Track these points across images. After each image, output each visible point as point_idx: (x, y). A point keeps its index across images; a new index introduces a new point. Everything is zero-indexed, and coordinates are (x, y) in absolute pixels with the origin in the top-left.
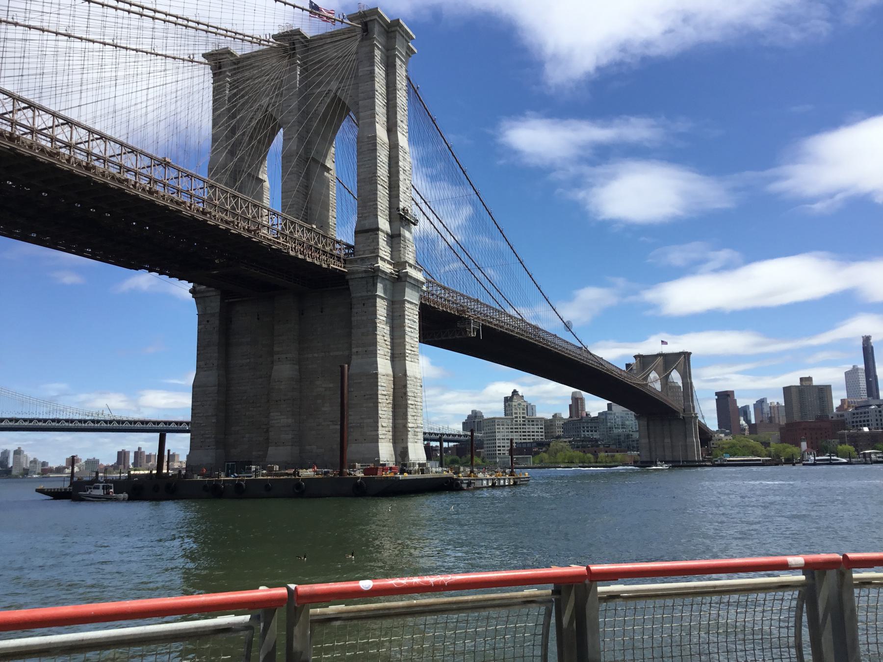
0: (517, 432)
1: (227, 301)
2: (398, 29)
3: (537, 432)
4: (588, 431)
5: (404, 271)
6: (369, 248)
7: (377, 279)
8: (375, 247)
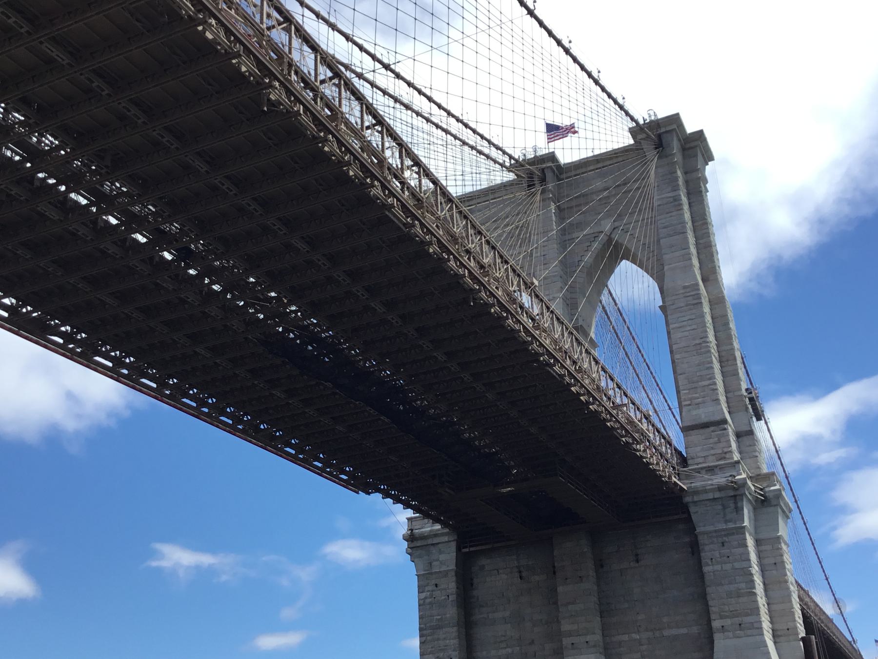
1: (467, 550)
2: (700, 143)
5: (772, 488)
6: (712, 452)
7: (742, 500)
8: (725, 450)
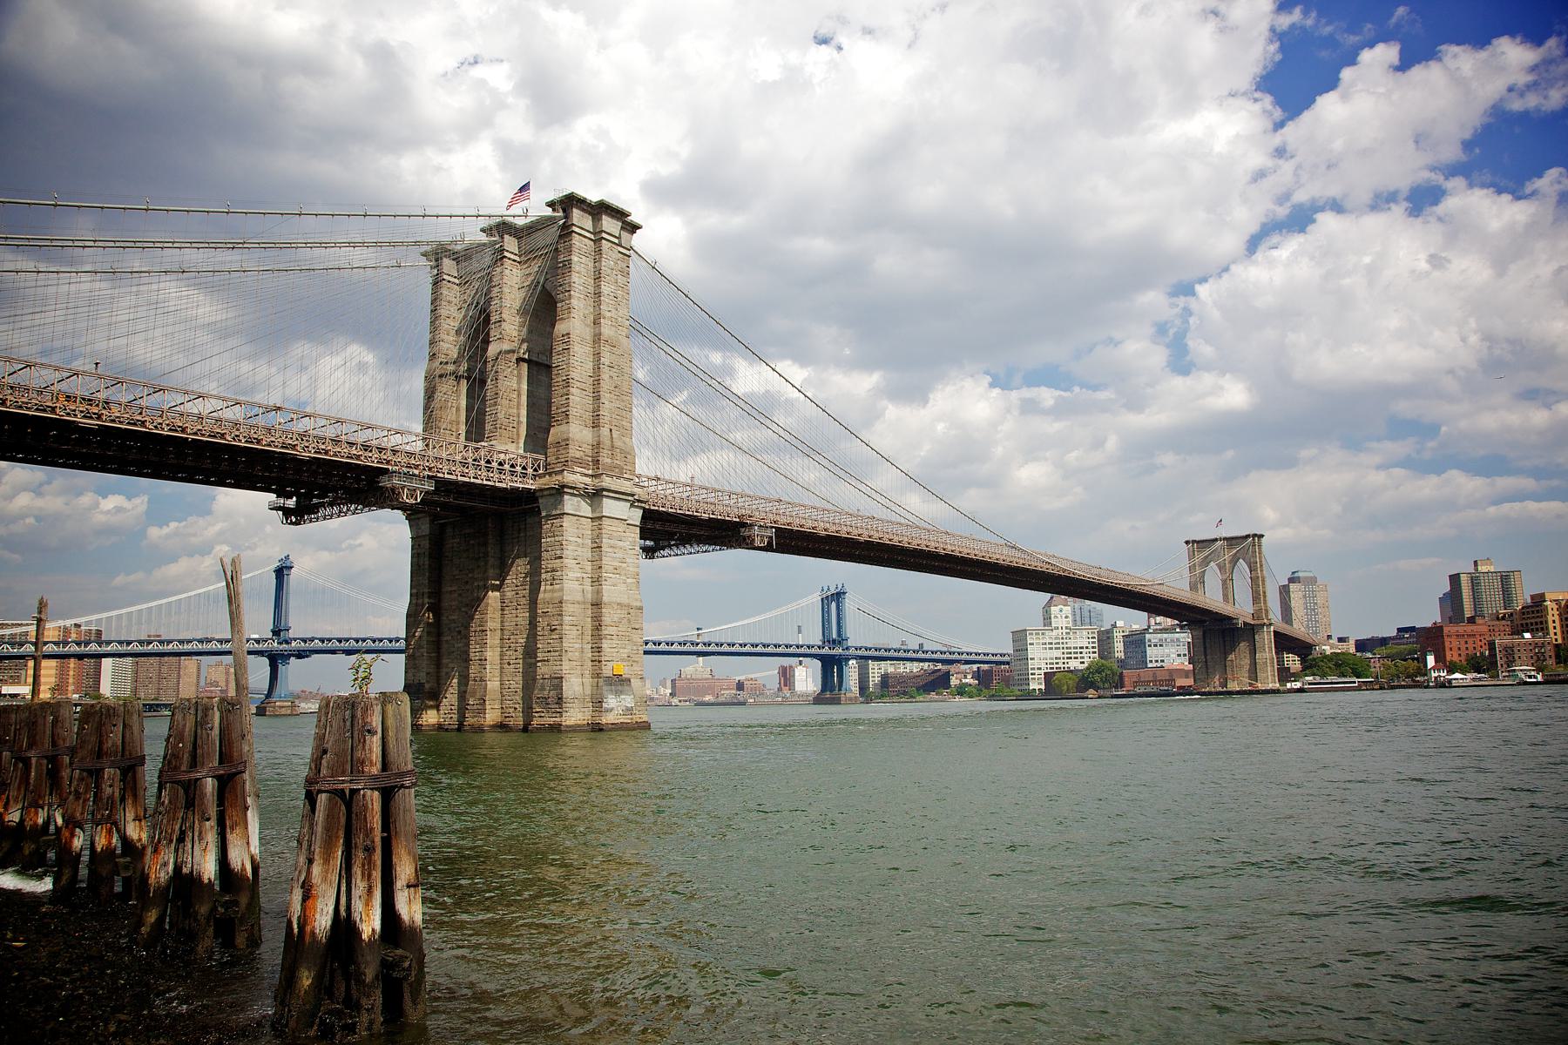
0: (1059, 648)
3: (1087, 648)
4: (1155, 646)
